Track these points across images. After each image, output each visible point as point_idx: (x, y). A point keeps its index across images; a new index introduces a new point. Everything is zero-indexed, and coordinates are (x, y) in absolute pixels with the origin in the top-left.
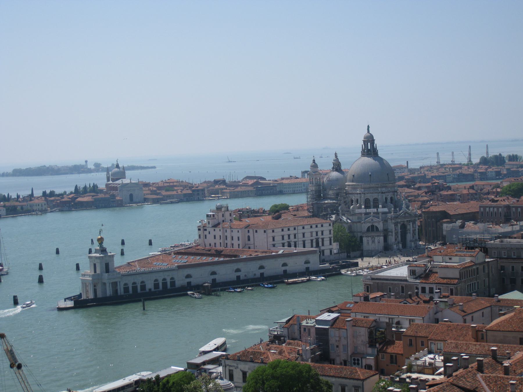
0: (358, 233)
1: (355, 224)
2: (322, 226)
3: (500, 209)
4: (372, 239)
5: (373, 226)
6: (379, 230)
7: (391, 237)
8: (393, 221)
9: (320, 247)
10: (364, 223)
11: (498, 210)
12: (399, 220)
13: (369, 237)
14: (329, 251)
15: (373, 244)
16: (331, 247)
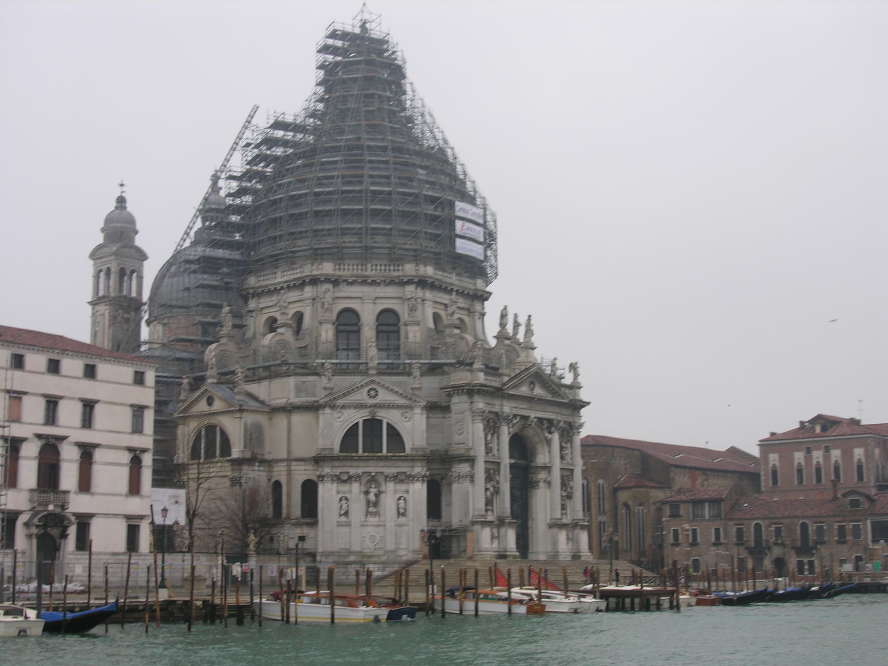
0: (295, 466)
1: (281, 421)
2: (90, 372)
3: (858, 453)
4: (367, 493)
5: (373, 425)
6: (404, 451)
7: (467, 484)
8: (480, 404)
9: (66, 492)
10: (333, 407)
11: (847, 454)
12: (507, 410)
13: (350, 479)
14: (121, 529)
15: (372, 520)
16: (135, 506)
